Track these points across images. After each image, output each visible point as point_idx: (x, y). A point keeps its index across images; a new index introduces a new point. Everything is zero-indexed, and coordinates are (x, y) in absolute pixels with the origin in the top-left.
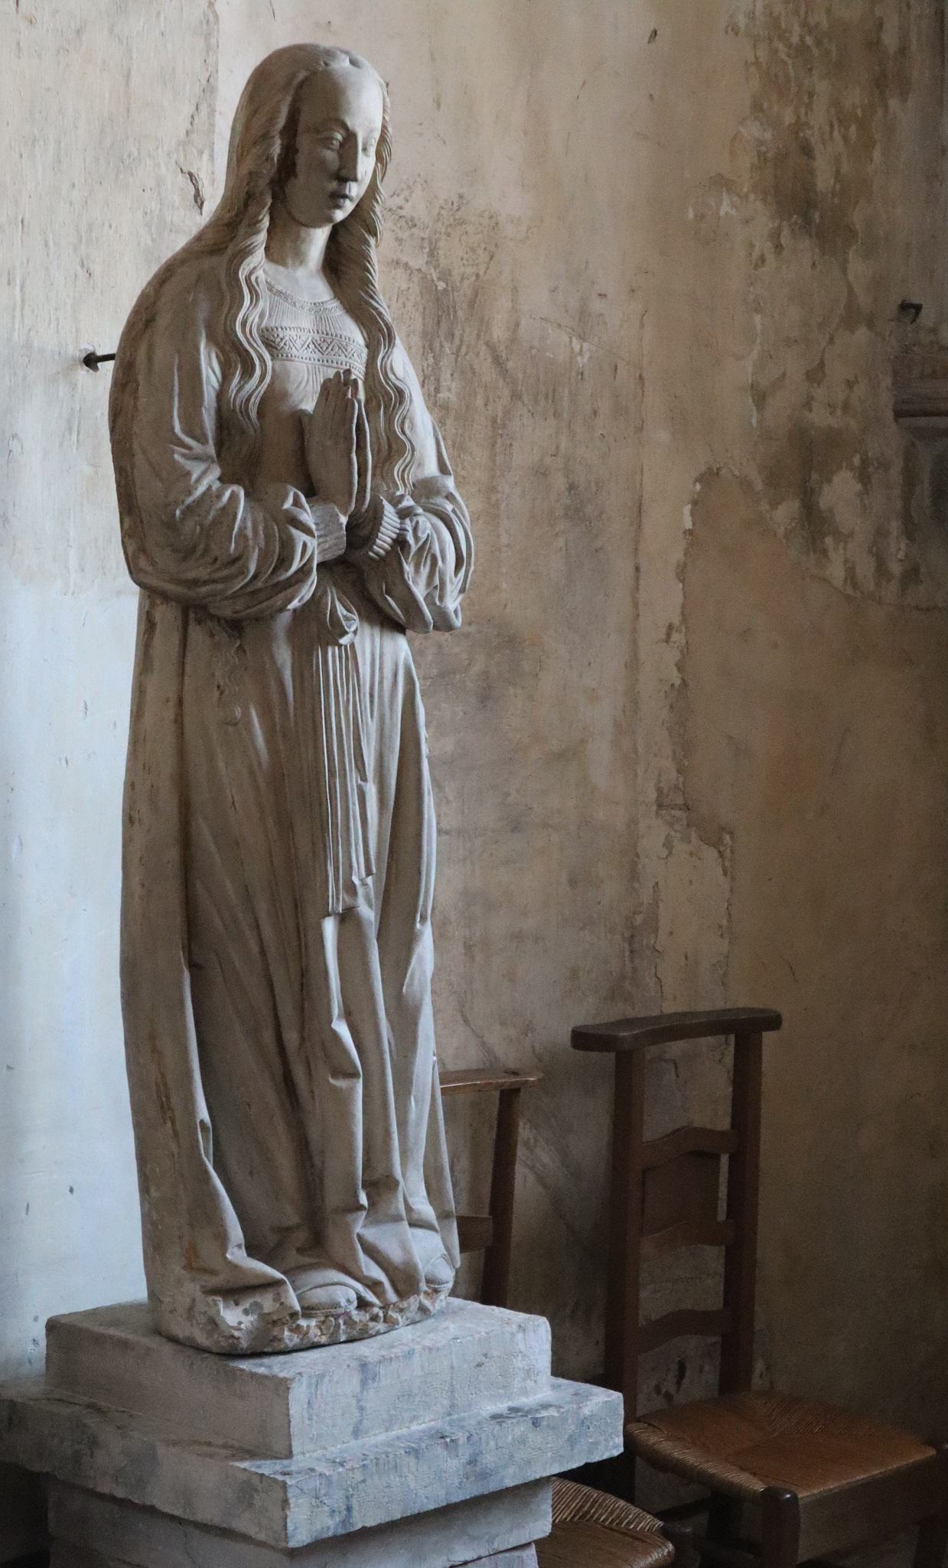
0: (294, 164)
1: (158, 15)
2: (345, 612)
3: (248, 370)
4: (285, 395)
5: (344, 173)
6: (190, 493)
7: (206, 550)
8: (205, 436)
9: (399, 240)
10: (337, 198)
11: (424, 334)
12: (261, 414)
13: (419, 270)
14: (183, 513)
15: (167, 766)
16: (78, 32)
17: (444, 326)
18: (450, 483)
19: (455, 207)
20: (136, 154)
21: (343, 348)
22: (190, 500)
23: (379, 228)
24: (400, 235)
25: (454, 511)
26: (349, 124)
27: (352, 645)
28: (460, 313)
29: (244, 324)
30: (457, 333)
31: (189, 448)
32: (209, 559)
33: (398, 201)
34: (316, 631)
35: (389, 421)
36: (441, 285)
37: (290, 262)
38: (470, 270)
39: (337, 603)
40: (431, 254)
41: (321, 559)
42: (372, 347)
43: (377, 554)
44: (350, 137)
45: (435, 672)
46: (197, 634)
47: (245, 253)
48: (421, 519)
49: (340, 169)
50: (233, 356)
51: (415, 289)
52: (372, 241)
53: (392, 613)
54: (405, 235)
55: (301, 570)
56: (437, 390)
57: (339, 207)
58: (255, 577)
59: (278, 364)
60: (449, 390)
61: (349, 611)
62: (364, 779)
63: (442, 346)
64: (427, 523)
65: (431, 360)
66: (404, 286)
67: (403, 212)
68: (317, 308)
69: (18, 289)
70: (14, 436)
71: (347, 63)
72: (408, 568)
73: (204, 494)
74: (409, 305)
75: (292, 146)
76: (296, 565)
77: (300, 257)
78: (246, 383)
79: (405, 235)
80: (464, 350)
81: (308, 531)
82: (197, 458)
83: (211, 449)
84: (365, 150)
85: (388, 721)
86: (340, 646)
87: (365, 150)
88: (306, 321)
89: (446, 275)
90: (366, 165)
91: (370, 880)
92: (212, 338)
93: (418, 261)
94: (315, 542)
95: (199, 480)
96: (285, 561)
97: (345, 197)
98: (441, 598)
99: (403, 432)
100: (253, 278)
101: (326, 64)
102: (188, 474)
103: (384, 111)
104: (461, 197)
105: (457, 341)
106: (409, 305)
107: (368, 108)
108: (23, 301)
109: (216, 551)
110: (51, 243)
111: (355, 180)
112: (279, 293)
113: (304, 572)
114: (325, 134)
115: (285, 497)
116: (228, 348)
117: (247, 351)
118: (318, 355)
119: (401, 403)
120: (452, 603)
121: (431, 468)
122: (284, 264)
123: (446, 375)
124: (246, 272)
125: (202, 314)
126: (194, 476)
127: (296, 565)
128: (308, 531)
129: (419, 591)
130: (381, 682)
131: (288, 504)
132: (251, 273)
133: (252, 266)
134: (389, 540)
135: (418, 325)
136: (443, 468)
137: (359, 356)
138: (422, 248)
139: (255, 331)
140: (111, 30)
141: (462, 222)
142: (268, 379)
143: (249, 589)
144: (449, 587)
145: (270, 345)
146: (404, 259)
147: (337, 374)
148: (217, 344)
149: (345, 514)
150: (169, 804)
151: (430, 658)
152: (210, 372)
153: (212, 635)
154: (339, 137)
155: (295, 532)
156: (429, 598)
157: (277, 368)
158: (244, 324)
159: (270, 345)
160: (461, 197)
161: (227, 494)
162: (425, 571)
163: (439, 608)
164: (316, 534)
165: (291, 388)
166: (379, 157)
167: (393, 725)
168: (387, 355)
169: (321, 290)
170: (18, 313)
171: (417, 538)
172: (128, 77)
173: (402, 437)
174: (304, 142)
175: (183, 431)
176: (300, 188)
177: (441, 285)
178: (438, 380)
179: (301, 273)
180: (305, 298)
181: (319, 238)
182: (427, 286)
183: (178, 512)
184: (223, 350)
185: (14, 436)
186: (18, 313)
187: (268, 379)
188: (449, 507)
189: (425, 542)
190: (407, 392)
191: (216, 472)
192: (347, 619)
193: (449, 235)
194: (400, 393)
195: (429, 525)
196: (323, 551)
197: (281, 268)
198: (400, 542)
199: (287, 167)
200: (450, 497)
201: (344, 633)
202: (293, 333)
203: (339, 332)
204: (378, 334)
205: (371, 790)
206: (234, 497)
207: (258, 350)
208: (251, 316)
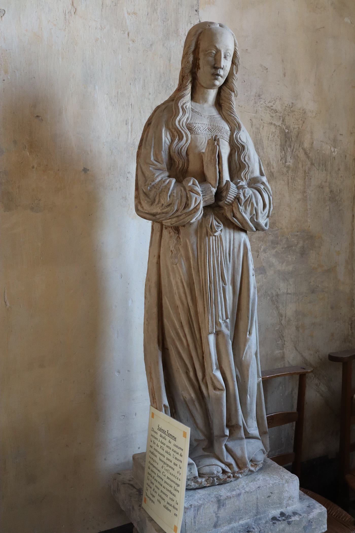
0: (199, 64)
1: (181, 40)
2: (217, 224)
3: (181, 138)
4: (196, 147)
5: (216, 66)
6: (153, 181)
7: (159, 201)
8: (162, 161)
9: (272, 117)
10: (216, 76)
11: (281, 145)
12: (187, 154)
13: (279, 126)
14: (151, 188)
15: (154, 278)
16: (151, 45)
17: (288, 143)
18: (264, 179)
19: (291, 106)
20: (173, 84)
21: (220, 131)
22: (153, 184)
23: (235, 89)
24: (272, 115)
25: (264, 188)
26: (217, 46)
27: (220, 236)
28: (293, 139)
29: (179, 122)
30: (292, 145)
31: (156, 165)
32: (160, 205)
33: (272, 104)
34: (204, 231)
35: (239, 156)
36: (287, 131)
37: (201, 101)
38: (296, 126)
39: (214, 220)
40: (283, 121)
41: (205, 205)
42: (232, 131)
43: (228, 202)
44: (218, 51)
45: (286, 246)
46: (165, 232)
47: (182, 97)
48: (246, 190)
49: (215, 64)
50: (176, 134)
51: (278, 132)
52: (233, 94)
53: (236, 224)
54: (274, 115)
55: (195, 208)
56: (286, 162)
57: (217, 79)
58: (177, 211)
59: (193, 136)
60: (290, 162)
61: (219, 223)
62: (225, 284)
63: (287, 149)
64: (249, 192)
65: (283, 153)
66: (274, 131)
67: (273, 108)
68: (211, 118)
69: (130, 127)
70: (129, 173)
71: (218, 26)
72: (242, 208)
73: (160, 181)
74: (276, 136)
75: (200, 59)
76: (192, 207)
77: (205, 101)
78: (180, 142)
79: (274, 115)
80: (295, 150)
81: (197, 193)
82: (159, 169)
83: (164, 166)
84: (225, 57)
85: (236, 262)
86: (215, 236)
87: (225, 57)
88: (206, 121)
89: (288, 127)
90: (226, 64)
91: (228, 321)
92: (168, 128)
93: (279, 123)
94: (201, 197)
95: (157, 176)
96: (187, 205)
97: (218, 75)
98: (257, 219)
99: (245, 161)
100: (184, 106)
101: (209, 26)
102: (154, 174)
103: (235, 45)
104: (292, 103)
105: (292, 147)
106: (276, 136)
107: (227, 43)
108: (132, 130)
109: (162, 201)
110: (142, 112)
111: (221, 68)
112: (196, 112)
113: (196, 209)
114: (209, 51)
115: (189, 181)
116: (173, 130)
117: (180, 131)
118: (210, 133)
119: (244, 150)
120: (263, 221)
121: (257, 173)
122: (199, 103)
123: (289, 158)
124: (182, 104)
125: (164, 120)
126: (157, 175)
127: (192, 207)
128: (197, 193)
129: (247, 217)
130: (233, 249)
131: (190, 184)
132: (184, 104)
133: (184, 102)
134: (233, 197)
135: (279, 143)
136: (262, 174)
137: (227, 133)
138: (280, 119)
139: (184, 124)
140: (163, 45)
141: (293, 111)
142: (189, 141)
143: (175, 215)
144: (260, 214)
145: (190, 129)
146: (274, 122)
147: (212, 137)
148: (169, 129)
149: (214, 188)
150: (154, 292)
151: (284, 242)
152: (166, 138)
153: (170, 233)
154: (214, 52)
155: (191, 193)
156: (252, 219)
157: (193, 137)
158: (179, 122)
159: (190, 129)
160: (292, 103)
161: (168, 181)
162: (249, 209)
163: (257, 222)
164: (201, 195)
165: (198, 144)
166: (233, 63)
167: (238, 264)
168: (238, 133)
169: (214, 112)
170: (130, 134)
171: (245, 197)
172: (170, 60)
173: (244, 162)
174: (201, 56)
175: (155, 160)
176: (203, 73)
177: (287, 131)
178: (286, 159)
179: (206, 105)
180: (207, 114)
181: (212, 94)
182: (282, 131)
183: (149, 188)
184: (171, 132)
185: (129, 173)
186: (130, 134)
187: (189, 141)
188: (262, 187)
189: (248, 198)
190: (246, 146)
191: (167, 174)
192: (218, 226)
193: (289, 115)
194: (243, 147)
195: (251, 192)
196: (205, 201)
197: (198, 104)
198: (237, 198)
199: (195, 66)
200: (263, 183)
201: (216, 231)
202: (200, 125)
203: (220, 125)
204: (235, 127)
205: (229, 288)
206: (170, 183)
207: (185, 131)
208: (182, 120)
